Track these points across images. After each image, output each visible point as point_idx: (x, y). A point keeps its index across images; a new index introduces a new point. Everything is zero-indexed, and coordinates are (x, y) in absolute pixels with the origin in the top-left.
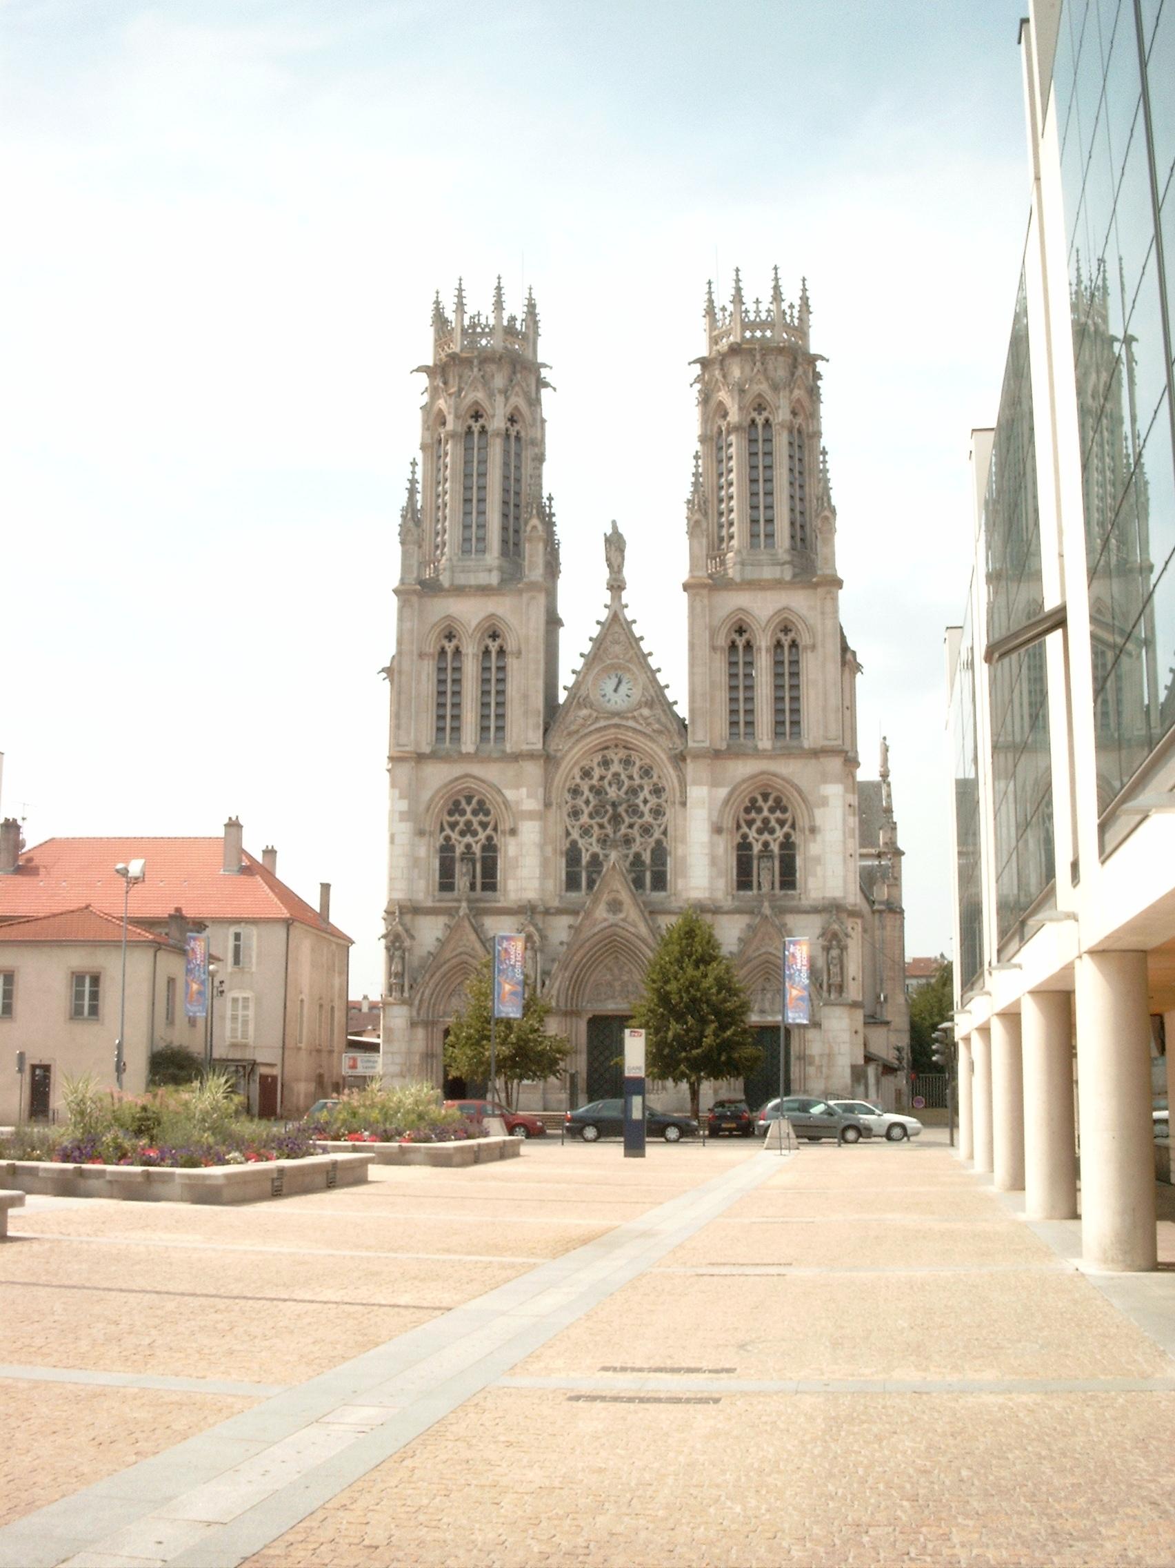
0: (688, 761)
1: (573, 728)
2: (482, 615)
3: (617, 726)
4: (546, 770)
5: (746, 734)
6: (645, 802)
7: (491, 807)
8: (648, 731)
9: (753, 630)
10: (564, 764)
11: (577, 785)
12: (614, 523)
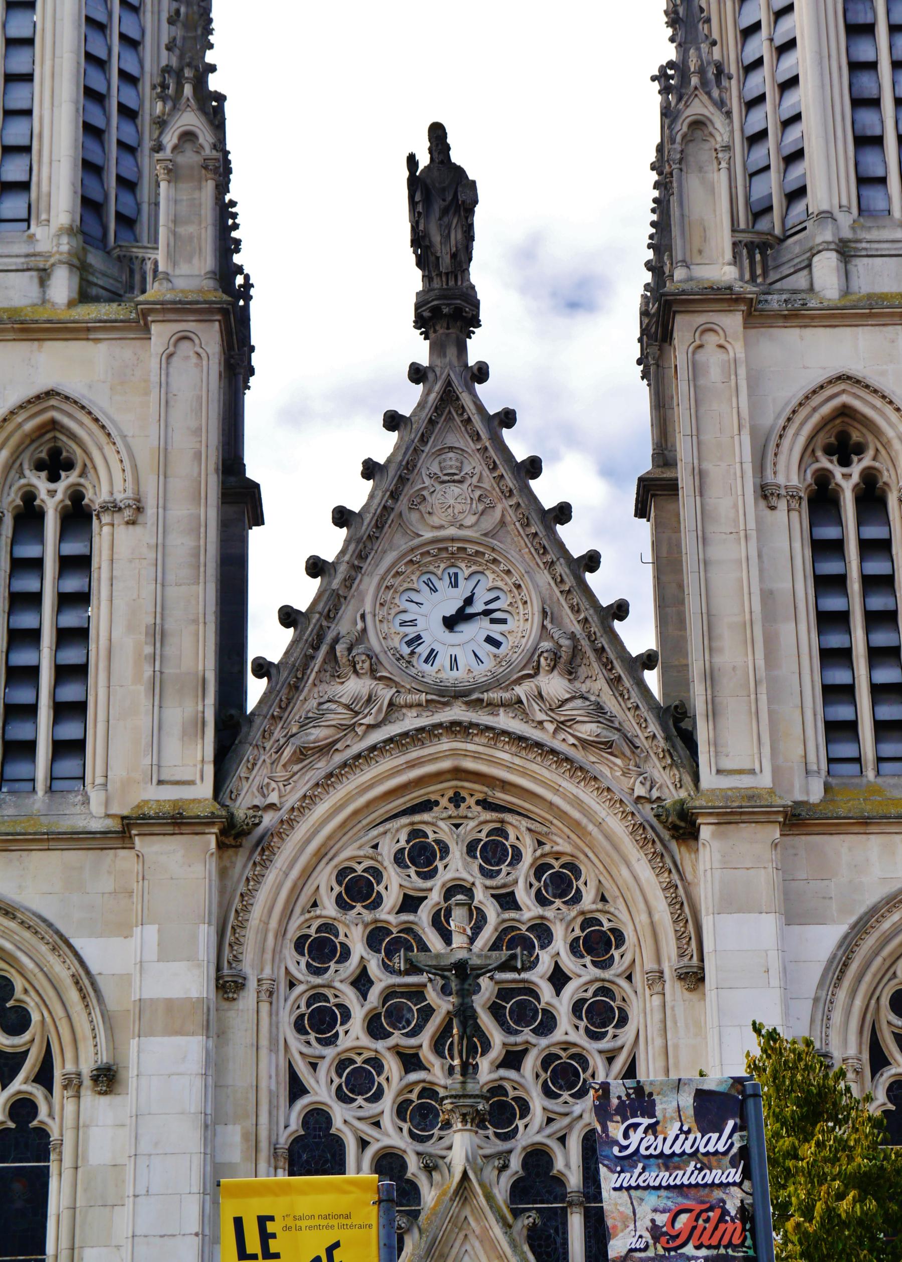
0: (705, 832)
1: (318, 734)
2: (14, 397)
3: (456, 728)
4: (223, 873)
5: (880, 760)
6: (559, 979)
7: (31, 1004)
8: (562, 744)
9: (887, 445)
10: (281, 860)
11: (328, 927)
12: (437, 133)
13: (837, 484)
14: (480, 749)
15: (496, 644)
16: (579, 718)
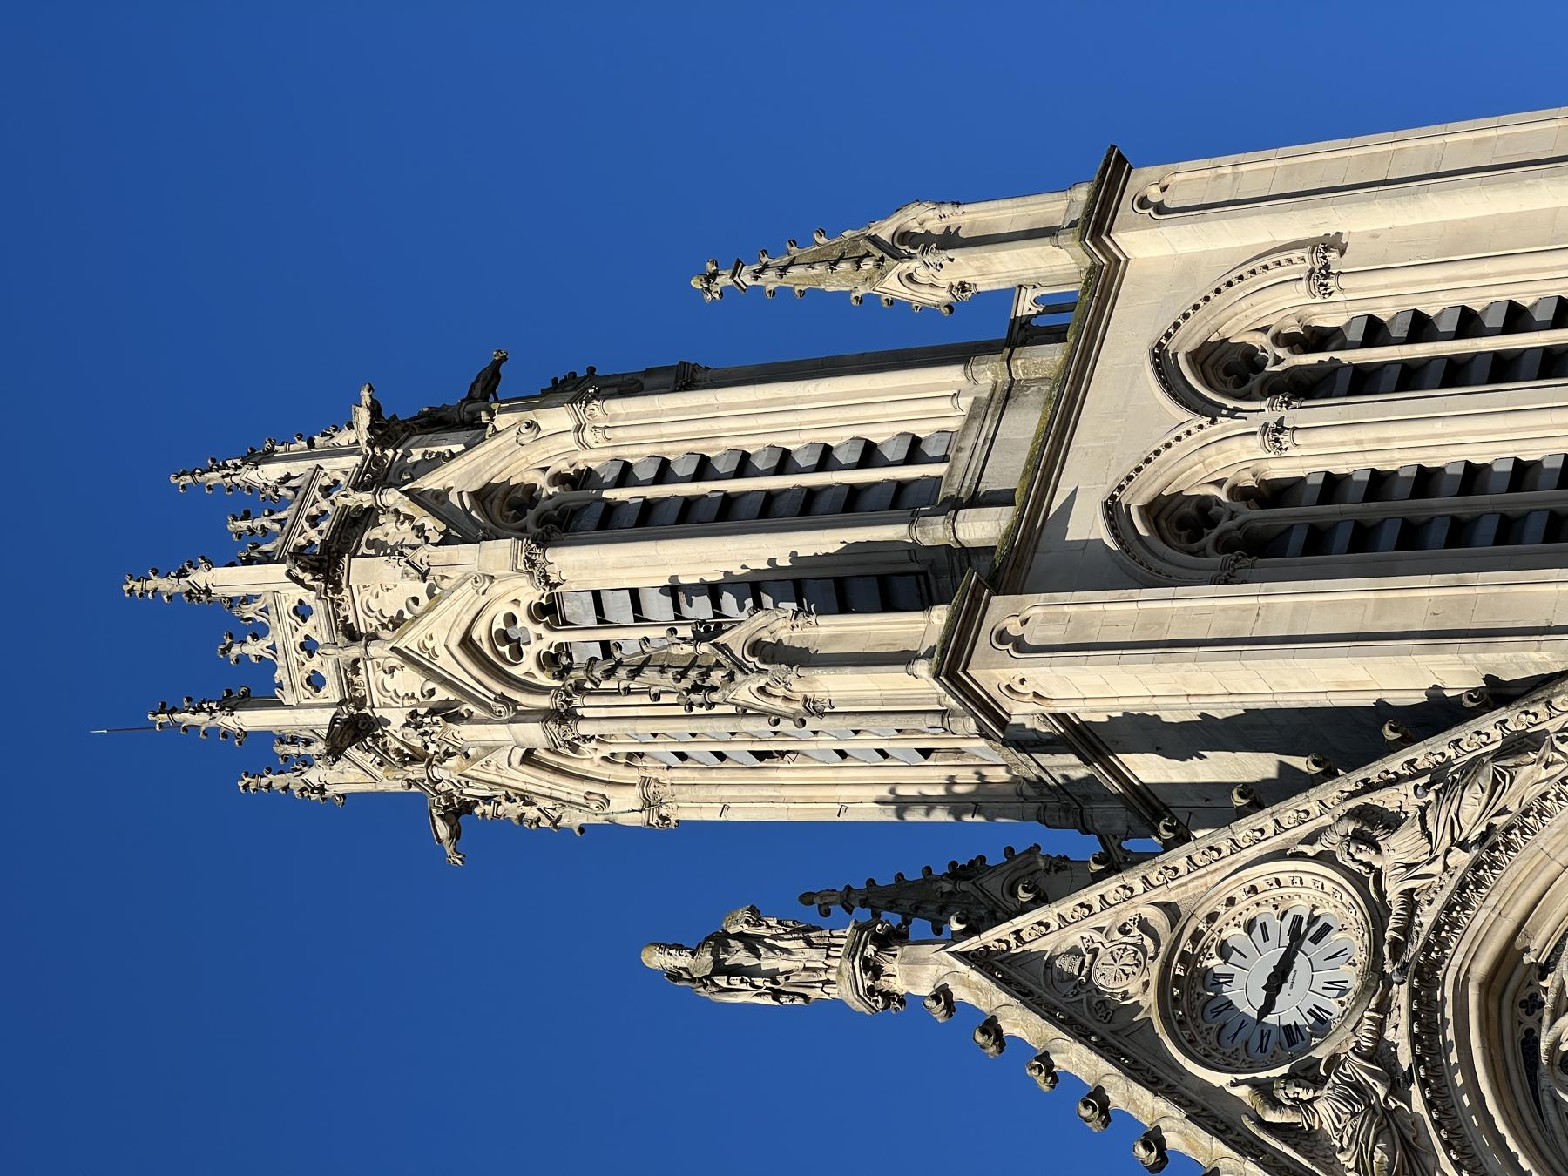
13: (1239, 529)
14: (1463, 948)
15: (1326, 928)
16: (1452, 814)
